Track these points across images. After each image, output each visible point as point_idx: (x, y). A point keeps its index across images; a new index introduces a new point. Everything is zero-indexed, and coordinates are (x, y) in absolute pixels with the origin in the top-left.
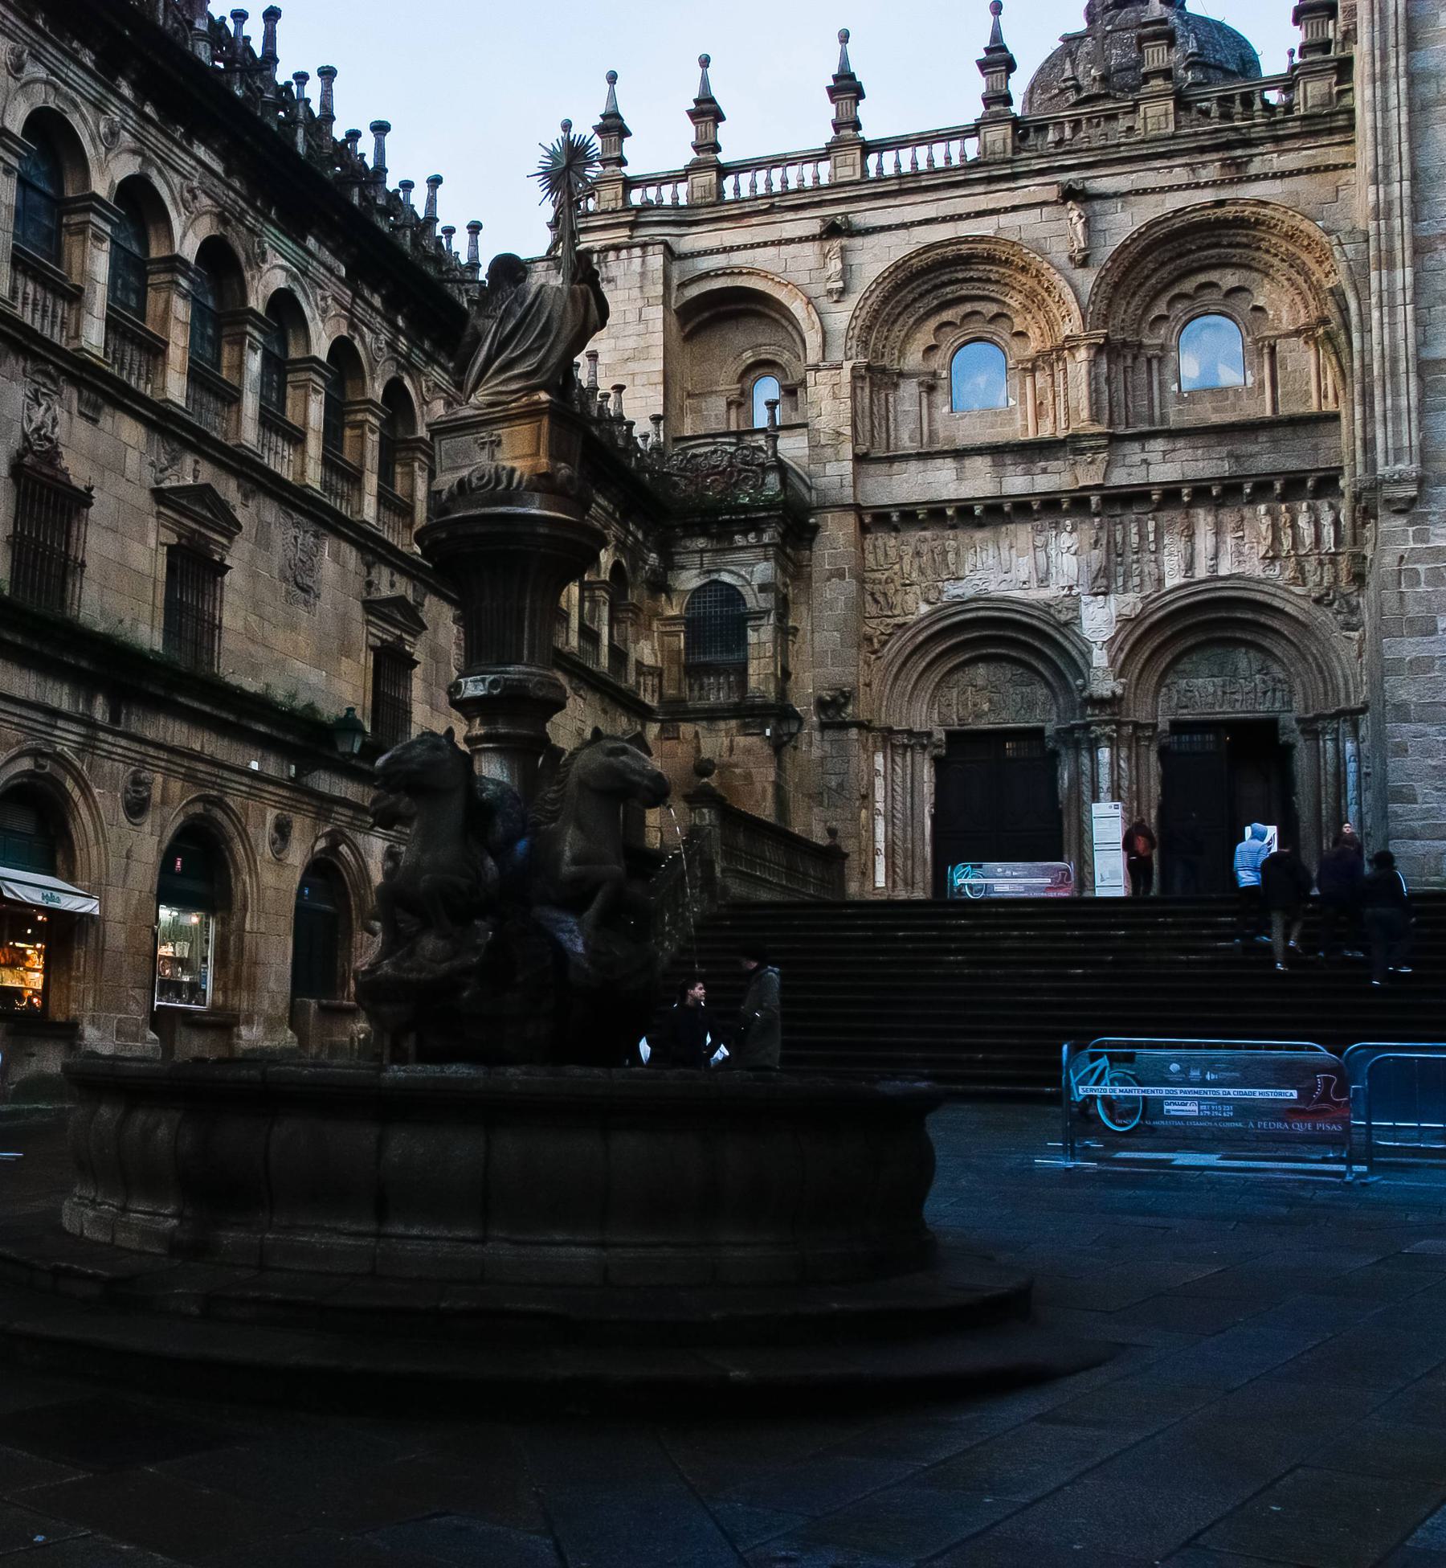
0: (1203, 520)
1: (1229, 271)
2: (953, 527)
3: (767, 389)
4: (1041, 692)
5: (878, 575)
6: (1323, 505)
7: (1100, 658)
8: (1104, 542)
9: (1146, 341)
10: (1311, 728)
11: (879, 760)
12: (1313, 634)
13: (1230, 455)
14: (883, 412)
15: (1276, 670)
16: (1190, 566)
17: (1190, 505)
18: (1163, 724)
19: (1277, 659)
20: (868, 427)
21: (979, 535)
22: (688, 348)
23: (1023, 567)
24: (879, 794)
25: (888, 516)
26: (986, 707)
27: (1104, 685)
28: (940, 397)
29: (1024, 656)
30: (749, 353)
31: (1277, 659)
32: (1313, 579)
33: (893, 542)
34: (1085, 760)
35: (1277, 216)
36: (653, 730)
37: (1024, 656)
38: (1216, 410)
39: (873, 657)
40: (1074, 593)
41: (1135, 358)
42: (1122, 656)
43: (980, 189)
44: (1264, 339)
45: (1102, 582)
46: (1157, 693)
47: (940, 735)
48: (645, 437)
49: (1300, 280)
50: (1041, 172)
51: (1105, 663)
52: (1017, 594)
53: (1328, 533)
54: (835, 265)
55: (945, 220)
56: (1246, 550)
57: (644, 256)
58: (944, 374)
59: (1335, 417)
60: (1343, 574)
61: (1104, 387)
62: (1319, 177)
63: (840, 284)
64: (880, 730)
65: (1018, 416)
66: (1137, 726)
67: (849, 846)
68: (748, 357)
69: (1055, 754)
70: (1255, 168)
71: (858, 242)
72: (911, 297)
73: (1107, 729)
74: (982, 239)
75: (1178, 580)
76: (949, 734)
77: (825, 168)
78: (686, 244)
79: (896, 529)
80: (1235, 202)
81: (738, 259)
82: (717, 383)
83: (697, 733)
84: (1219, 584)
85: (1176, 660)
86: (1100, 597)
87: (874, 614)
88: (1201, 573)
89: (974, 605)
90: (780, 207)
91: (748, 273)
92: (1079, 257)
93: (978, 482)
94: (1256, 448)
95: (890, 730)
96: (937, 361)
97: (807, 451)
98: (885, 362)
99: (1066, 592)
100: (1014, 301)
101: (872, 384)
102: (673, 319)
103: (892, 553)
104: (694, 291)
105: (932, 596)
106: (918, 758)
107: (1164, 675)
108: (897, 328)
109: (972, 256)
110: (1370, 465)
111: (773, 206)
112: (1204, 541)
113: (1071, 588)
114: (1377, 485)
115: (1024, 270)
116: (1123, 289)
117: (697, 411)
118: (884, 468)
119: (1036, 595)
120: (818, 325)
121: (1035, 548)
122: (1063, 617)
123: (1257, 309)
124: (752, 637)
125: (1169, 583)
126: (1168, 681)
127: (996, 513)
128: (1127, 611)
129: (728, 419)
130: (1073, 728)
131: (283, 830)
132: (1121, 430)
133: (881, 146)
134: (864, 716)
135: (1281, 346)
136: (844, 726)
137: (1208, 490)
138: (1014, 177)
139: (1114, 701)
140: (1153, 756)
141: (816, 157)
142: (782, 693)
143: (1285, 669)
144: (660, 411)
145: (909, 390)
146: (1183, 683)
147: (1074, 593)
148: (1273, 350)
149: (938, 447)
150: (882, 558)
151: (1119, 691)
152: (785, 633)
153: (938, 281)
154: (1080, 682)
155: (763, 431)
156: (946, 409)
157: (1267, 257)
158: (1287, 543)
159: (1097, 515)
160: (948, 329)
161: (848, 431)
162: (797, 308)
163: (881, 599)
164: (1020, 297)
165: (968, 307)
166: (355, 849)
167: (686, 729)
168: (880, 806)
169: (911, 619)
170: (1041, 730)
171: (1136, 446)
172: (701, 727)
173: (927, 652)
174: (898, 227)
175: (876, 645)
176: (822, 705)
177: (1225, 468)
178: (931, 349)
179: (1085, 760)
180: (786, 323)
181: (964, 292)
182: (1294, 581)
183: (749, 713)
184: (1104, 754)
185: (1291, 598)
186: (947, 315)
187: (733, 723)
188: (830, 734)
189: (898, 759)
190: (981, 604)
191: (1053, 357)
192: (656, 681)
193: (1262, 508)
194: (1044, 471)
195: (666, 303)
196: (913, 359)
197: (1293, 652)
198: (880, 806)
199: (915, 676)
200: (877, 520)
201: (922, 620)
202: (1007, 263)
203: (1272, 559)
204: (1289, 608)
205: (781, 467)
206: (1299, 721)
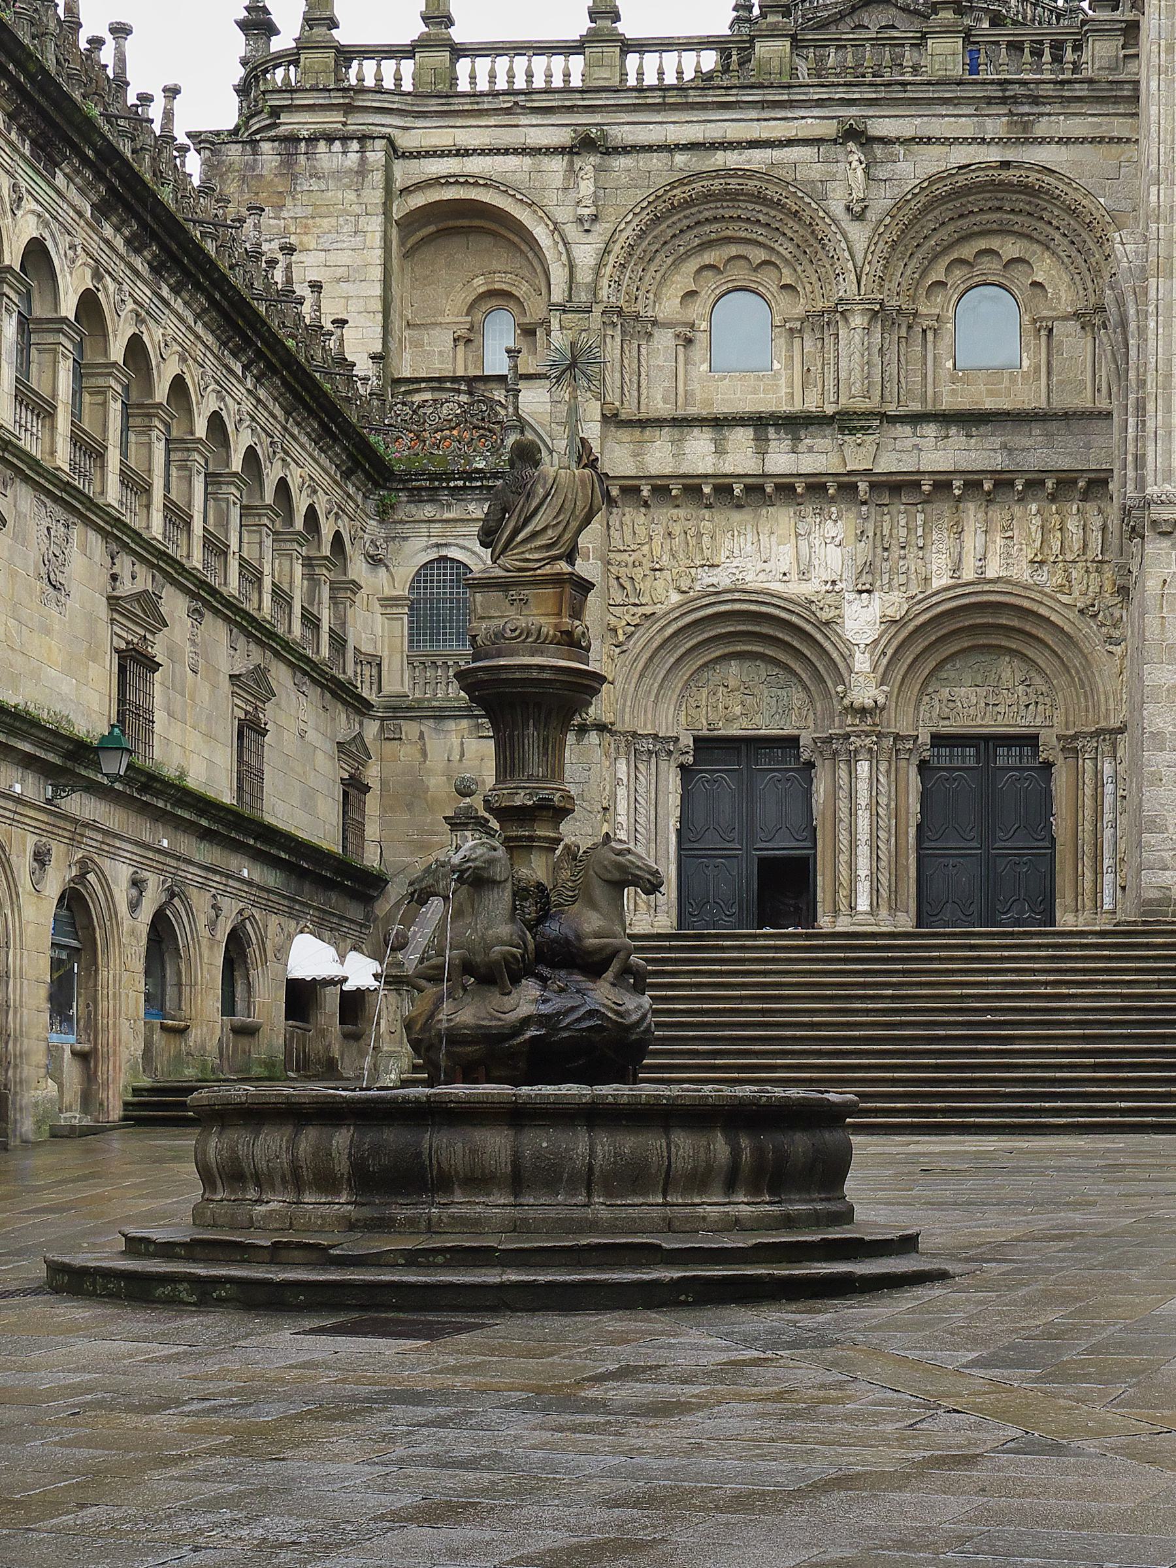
0: (972, 511)
1: (1010, 240)
2: (709, 506)
4: (797, 696)
5: (625, 556)
6: (1091, 508)
7: (862, 662)
8: (871, 534)
9: (922, 310)
10: (1070, 746)
11: (622, 766)
12: (1076, 645)
13: (1004, 446)
14: (635, 366)
15: (1038, 680)
16: (957, 568)
17: (959, 499)
18: (925, 738)
19: (1040, 670)
20: (619, 384)
21: (736, 516)
22: (408, 265)
23: (784, 556)
24: (622, 807)
25: (638, 490)
26: (738, 710)
27: (865, 692)
28: (698, 351)
29: (782, 657)
30: (480, 280)
31: (1040, 670)
33: (642, 519)
34: (843, 773)
35: (1061, 186)
36: (372, 729)
37: (782, 657)
38: (990, 393)
39: (618, 650)
40: (837, 588)
41: (910, 327)
42: (885, 661)
43: (753, 114)
44: (1042, 319)
46: (919, 701)
47: (687, 741)
48: (366, 379)
49: (1079, 260)
50: (820, 103)
53: (1096, 538)
54: (586, 187)
56: (1014, 551)
57: (362, 151)
58: (704, 326)
59: (1109, 415)
60: (1108, 586)
61: (877, 359)
62: (1103, 149)
63: (592, 210)
64: (623, 734)
65: (782, 382)
66: (897, 737)
68: (480, 284)
69: (811, 765)
70: (1041, 128)
72: (670, 232)
73: (868, 741)
74: (751, 174)
75: (945, 581)
76: (697, 739)
77: (577, 63)
78: (406, 141)
79: (646, 505)
80: (1019, 165)
81: (475, 165)
82: (442, 313)
83: (422, 733)
84: (986, 588)
85: (939, 666)
86: (865, 595)
87: (619, 601)
88: (968, 575)
89: (729, 597)
90: (524, 107)
91: (485, 185)
92: (857, 209)
93: (740, 456)
94: (1028, 442)
95: (634, 734)
96: (696, 311)
97: (548, 407)
98: (639, 307)
99: (829, 587)
100: (785, 248)
101: (623, 333)
102: (394, 233)
103: (641, 531)
104: (418, 200)
105: (684, 584)
106: (663, 765)
107: (925, 683)
108: (652, 268)
109: (741, 192)
112: (972, 541)
113: (834, 582)
116: (901, 248)
117: (418, 344)
119: (796, 589)
120: (564, 258)
121: (798, 535)
122: (824, 616)
123: (1035, 284)
125: (936, 584)
126: (930, 690)
127: (759, 493)
128: (888, 612)
129: (455, 358)
130: (830, 739)
131: (41, 858)
132: (891, 409)
133: (641, 46)
134: (607, 718)
135: (1058, 327)
137: (980, 484)
138: (790, 104)
140: (913, 772)
141: (567, 49)
143: (1048, 681)
144: (378, 348)
145: (664, 339)
146: (945, 693)
147: (837, 588)
148: (1051, 330)
149: (693, 411)
150: (628, 537)
151: (881, 700)
153: (701, 217)
154: (840, 688)
155: (502, 379)
156: (705, 367)
157: (1049, 229)
158: (1056, 546)
159: (864, 503)
160: (709, 274)
162: (541, 233)
163: (628, 585)
164: (787, 244)
165: (733, 250)
167: (410, 729)
168: (622, 819)
169: (659, 609)
170: (796, 739)
171: (908, 429)
172: (427, 726)
173: (676, 647)
175: (621, 638)
177: (998, 461)
178: (691, 294)
179: (843, 773)
180: (524, 247)
181: (729, 233)
182: (1060, 589)
184: (863, 768)
185: (1058, 607)
186: (709, 257)
187: (465, 723)
189: (641, 767)
190: (737, 596)
191: (824, 321)
192: (374, 672)
193: (1034, 507)
194: (810, 449)
195: (387, 213)
196: (669, 306)
197: (1057, 663)
199: (661, 675)
201: (672, 610)
202: (778, 205)
203: (1037, 564)
204: (1054, 618)
206: (1059, 738)
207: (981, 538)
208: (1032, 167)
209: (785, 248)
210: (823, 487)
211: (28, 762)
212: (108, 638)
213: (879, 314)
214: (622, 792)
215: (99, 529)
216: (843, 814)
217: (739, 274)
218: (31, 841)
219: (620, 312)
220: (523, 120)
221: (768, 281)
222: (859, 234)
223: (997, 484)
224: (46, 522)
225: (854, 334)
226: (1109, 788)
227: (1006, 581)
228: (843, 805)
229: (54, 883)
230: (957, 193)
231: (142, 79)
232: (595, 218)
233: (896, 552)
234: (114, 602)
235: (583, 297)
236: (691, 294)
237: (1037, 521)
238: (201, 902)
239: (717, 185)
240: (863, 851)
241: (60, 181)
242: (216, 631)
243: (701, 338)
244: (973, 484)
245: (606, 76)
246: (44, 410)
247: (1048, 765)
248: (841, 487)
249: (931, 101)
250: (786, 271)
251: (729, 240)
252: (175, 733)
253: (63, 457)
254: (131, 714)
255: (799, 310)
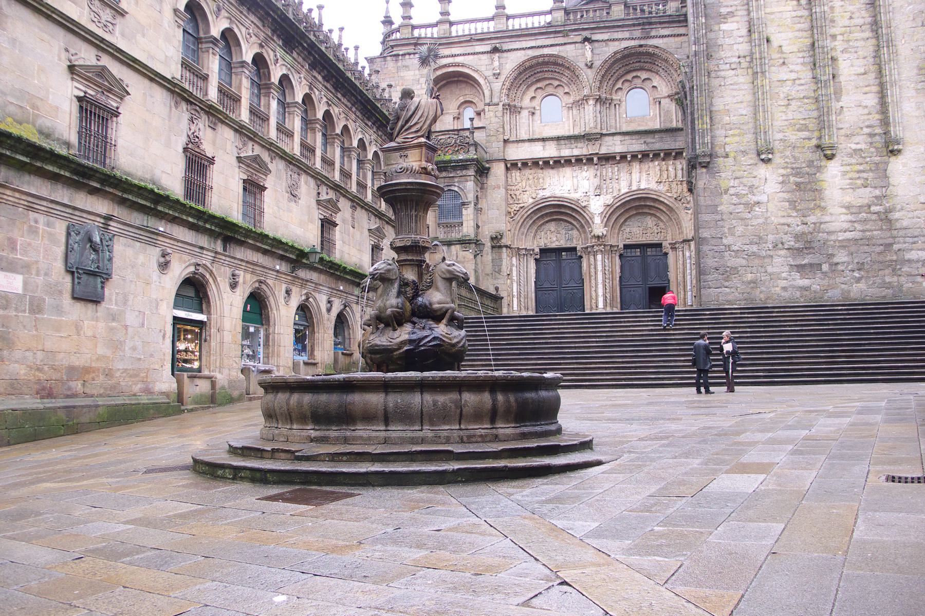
0: (636, 166)
1: (644, 72)
3: (469, 113)
5: (513, 188)
6: (678, 162)
7: (597, 220)
9: (614, 98)
10: (674, 247)
11: (514, 259)
15: (661, 224)
16: (630, 185)
17: (630, 162)
18: (621, 246)
19: (662, 221)
24: (514, 273)
25: (517, 164)
28: (537, 116)
31: (662, 221)
32: (674, 191)
43: (552, 36)
45: (598, 191)
46: (618, 234)
47: (537, 250)
50: (575, 30)
51: (599, 222)
52: (566, 195)
54: (496, 64)
55: (538, 47)
58: (538, 108)
59: (682, 129)
60: (685, 190)
61: (598, 115)
66: (611, 246)
67: (503, 294)
68: (462, 99)
69: (581, 257)
71: (505, 55)
75: (626, 190)
76: (540, 250)
85: (625, 221)
88: (634, 188)
92: (589, 64)
93: (551, 151)
96: (535, 103)
100: (565, 80)
103: (518, 178)
104: (439, 73)
107: (621, 226)
110: (694, 149)
111: (471, 39)
112: (635, 176)
114: (697, 157)
115: (568, 68)
118: (516, 145)
119: (574, 196)
122: (583, 204)
124: (464, 212)
125: (623, 191)
127: (558, 163)
130: (587, 248)
132: (604, 132)
133: (514, 17)
134: (509, 243)
135: (663, 101)
136: (500, 247)
137: (637, 156)
139: (604, 236)
140: (617, 258)
142: (477, 235)
143: (665, 225)
145: (525, 113)
152: (478, 211)
155: (468, 129)
158: (665, 176)
160: (539, 91)
161: (501, 130)
162: (481, 81)
165: (547, 82)
166: (315, 299)
168: (515, 278)
169: (526, 205)
174: (520, 49)
176: (492, 239)
177: (643, 147)
178: (533, 98)
183: (464, 242)
184: (599, 257)
186: (539, 85)
188: (496, 250)
191: (580, 103)
196: (526, 102)
198: (515, 278)
200: (512, 166)
202: (562, 65)
204: (666, 201)
205: (476, 145)
207: (638, 175)
208: (650, 46)
209: (565, 80)
210: (581, 160)
211: (282, 258)
212: (317, 215)
213: (598, 100)
214: (514, 269)
215: (312, 176)
216: (593, 273)
217: (550, 90)
218: (284, 287)
219: (509, 105)
220: (474, 43)
221: (560, 91)
222: (590, 74)
223: (643, 156)
224: (290, 173)
225: (590, 108)
226: (688, 261)
227: (648, 189)
228: (592, 270)
229: (295, 302)
230: (624, 57)
231: (348, 42)
232: (499, 74)
233: (608, 181)
234: (319, 202)
235: (495, 100)
236: (533, 98)
237: (658, 168)
238: (357, 309)
239: (541, 60)
240: (600, 286)
241: (295, 55)
242: (361, 214)
243: (537, 112)
244: (634, 157)
245: (502, 27)
246: (290, 135)
247: (666, 254)
248: (588, 160)
249: (614, 27)
250: (566, 87)
251: (545, 79)
252: (346, 249)
253: (297, 151)
254: (326, 241)
255: (571, 101)
